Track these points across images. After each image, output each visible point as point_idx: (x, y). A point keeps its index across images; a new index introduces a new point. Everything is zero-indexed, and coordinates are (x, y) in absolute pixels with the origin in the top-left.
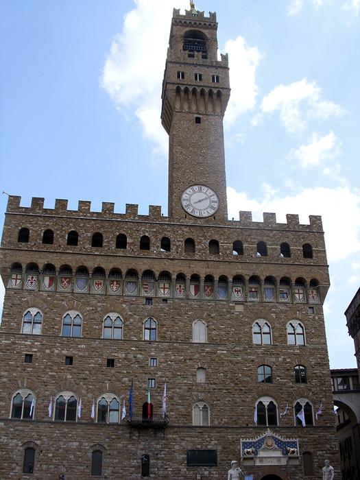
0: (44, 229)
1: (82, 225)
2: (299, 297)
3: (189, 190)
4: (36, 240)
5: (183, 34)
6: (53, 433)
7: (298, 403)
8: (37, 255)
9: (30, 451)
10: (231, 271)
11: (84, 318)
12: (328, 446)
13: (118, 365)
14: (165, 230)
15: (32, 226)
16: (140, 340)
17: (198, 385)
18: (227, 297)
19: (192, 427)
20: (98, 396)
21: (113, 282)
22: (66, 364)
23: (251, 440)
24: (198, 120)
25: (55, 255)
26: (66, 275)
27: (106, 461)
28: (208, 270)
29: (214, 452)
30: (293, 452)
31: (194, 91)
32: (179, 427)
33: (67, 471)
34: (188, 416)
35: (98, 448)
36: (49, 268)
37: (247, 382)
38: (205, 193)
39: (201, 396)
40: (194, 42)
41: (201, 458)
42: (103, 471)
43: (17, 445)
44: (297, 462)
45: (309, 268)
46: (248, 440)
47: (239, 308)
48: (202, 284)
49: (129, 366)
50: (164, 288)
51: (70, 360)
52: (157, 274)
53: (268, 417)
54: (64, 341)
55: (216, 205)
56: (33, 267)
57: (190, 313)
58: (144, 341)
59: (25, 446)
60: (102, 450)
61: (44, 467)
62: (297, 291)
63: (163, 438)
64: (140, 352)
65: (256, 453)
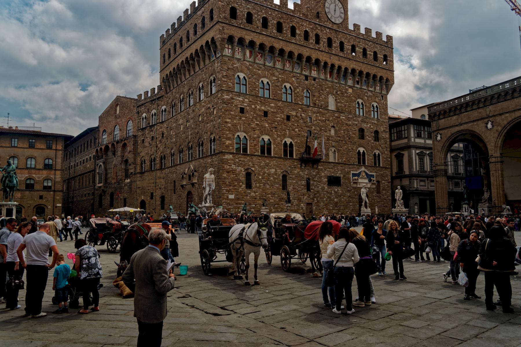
1: (270, 13)
2: (378, 88)
4: (242, 20)
6: (261, 163)
9: (248, 175)
10: (351, 65)
13: (293, 120)
14: (317, 28)
15: (239, 7)
19: (330, 163)
23: (355, 172)
25: (255, 34)
27: (289, 181)
28: (339, 62)
29: (340, 177)
30: (374, 181)
32: (323, 162)
34: (327, 155)
35: (285, 173)
36: (252, 44)
37: (354, 138)
41: (334, 181)
42: (288, 187)
43: (241, 171)
44: (374, 186)
45: (385, 71)
47: (350, 90)
48: (335, 71)
50: (314, 70)
51: (266, 114)
53: (361, 158)
55: (343, 16)
56: (241, 41)
58: (305, 105)
60: (287, 174)
61: (258, 185)
63: (317, 168)
65: (358, 179)
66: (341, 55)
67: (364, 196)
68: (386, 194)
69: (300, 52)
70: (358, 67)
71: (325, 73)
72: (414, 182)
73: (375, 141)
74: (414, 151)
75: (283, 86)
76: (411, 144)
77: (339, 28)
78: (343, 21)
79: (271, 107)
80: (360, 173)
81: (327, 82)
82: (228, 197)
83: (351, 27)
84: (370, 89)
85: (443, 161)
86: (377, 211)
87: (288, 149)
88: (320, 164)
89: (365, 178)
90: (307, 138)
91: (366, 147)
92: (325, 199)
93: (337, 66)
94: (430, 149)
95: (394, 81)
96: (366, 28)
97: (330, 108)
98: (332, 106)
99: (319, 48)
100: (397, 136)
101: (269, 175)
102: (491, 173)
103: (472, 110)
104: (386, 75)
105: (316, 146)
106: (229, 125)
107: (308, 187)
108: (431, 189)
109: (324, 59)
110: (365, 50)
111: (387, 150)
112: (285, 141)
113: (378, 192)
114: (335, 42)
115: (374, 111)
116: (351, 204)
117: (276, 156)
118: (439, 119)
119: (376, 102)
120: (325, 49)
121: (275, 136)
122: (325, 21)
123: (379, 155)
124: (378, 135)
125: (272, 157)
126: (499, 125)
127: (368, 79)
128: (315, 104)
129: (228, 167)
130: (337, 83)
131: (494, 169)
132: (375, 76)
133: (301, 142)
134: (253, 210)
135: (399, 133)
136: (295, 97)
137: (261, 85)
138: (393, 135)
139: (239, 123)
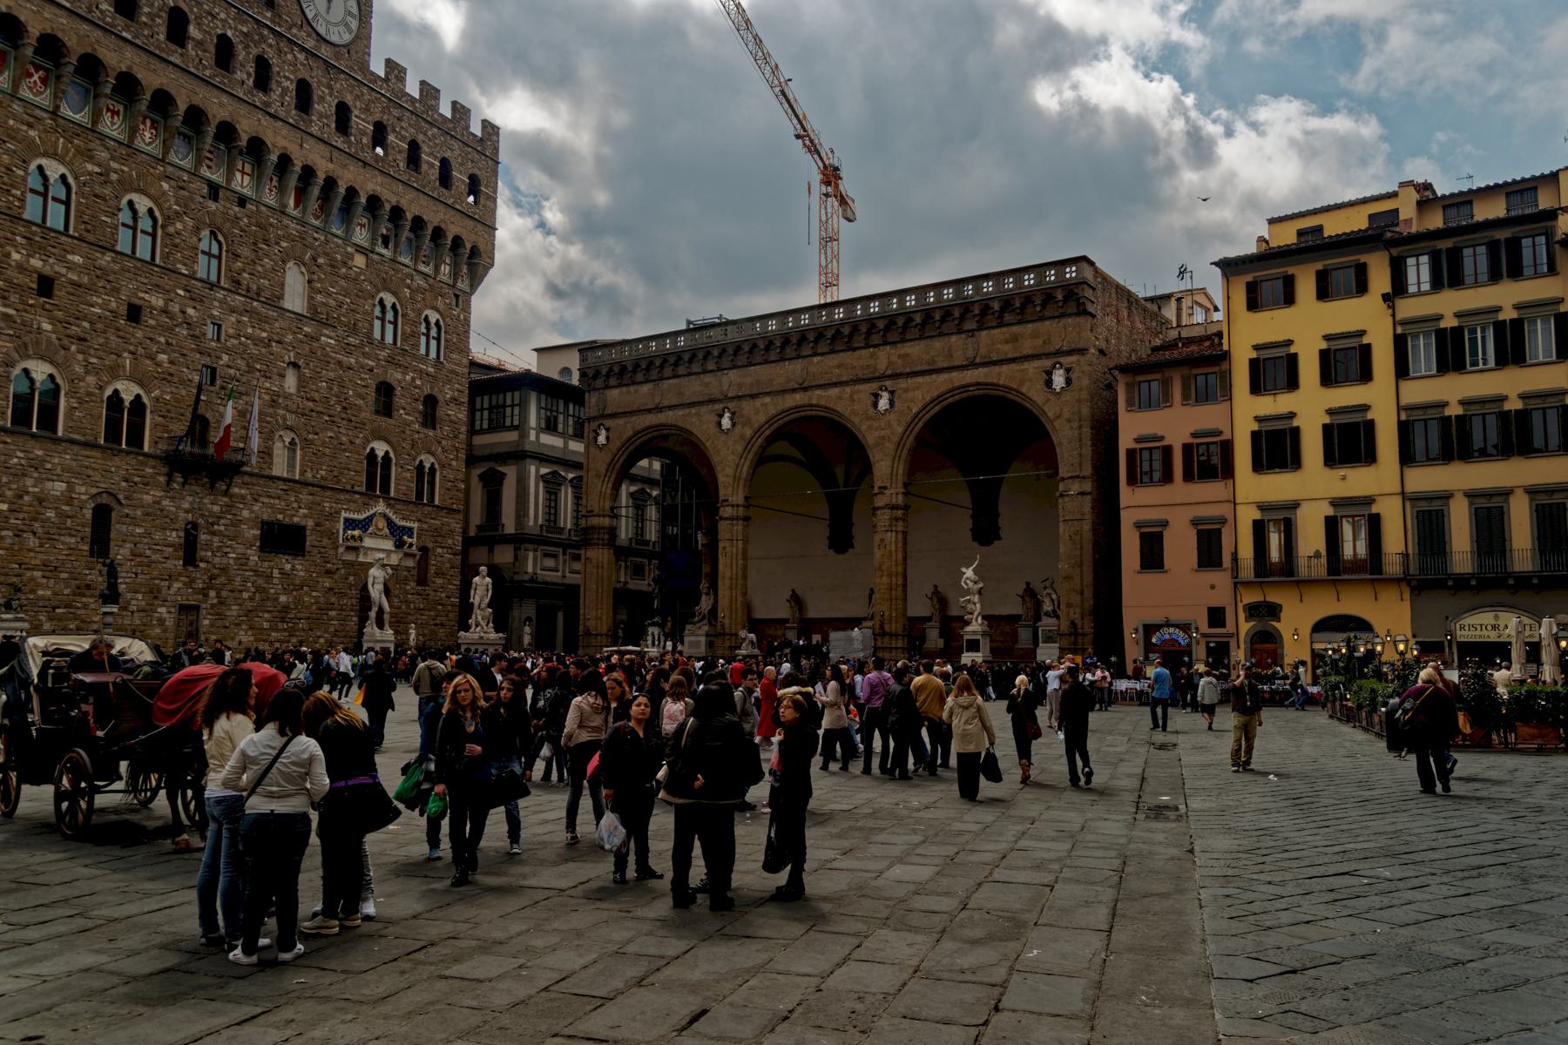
2: (445, 269)
6: (11, 456)
10: (370, 184)
11: (78, 186)
14: (263, 39)
16: (192, 277)
17: (288, 397)
18: (347, 231)
19: (272, 478)
20: (108, 383)
21: (145, 118)
27: (118, 529)
28: (331, 166)
29: (304, 528)
30: (411, 545)
32: (251, 475)
33: (41, 545)
34: (266, 454)
35: (105, 500)
37: (360, 408)
39: (291, 419)
41: (281, 539)
42: (113, 550)
44: (410, 563)
45: (471, 223)
46: (352, 516)
47: (360, 261)
48: (316, 191)
49: (170, 329)
50: (243, 173)
51: (46, 285)
53: (377, 474)
54: (34, 233)
55: (354, 24)
57: (284, 244)
60: (114, 505)
63: (226, 493)
64: (191, 303)
66: (339, 145)
67: (376, 592)
68: (444, 587)
69: (196, 101)
70: (391, 195)
71: (282, 190)
72: (526, 558)
73: (425, 425)
74: (533, 469)
75: (124, 202)
76: (527, 448)
77: (338, 60)
78: (352, 42)
79: (71, 267)
80: (370, 520)
81: (286, 221)
83: (378, 68)
84: (422, 268)
85: (608, 504)
86: (413, 636)
87: (123, 422)
88: (238, 480)
89: (385, 537)
90: (200, 389)
92: (245, 595)
93: (321, 176)
94: (577, 466)
95: (492, 259)
96: (423, 83)
97: (287, 305)
98: (295, 297)
99: (265, 103)
100: (490, 420)
101: (40, 501)
102: (721, 545)
103: (690, 374)
104: (473, 238)
105: (228, 419)
107: (190, 551)
108: (572, 579)
109: (282, 143)
110: (414, 147)
111: (457, 458)
112: (116, 392)
113: (422, 580)
114: (322, 99)
115: (427, 335)
116: (333, 613)
117: (76, 437)
118: (607, 387)
119: (438, 310)
120: (288, 112)
121: (78, 369)
122: (295, 25)
123: (432, 469)
124: (434, 409)
125: (60, 440)
126: (748, 422)
127: (418, 237)
128: (238, 283)
130: (317, 229)
131: (728, 536)
132: (438, 233)
133: (177, 401)
135: (497, 410)
136: (164, 245)
137: (34, 182)
138: (478, 414)
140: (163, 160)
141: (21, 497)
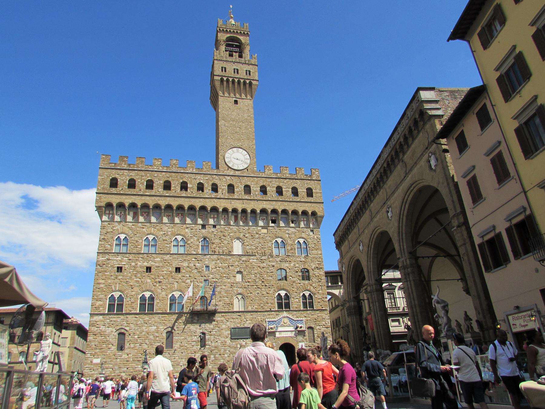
0: (128, 178)
1: (156, 175)
3: (230, 150)
5: (225, 38)
7: (304, 294)
8: (124, 197)
9: (122, 335)
12: (324, 323)
13: (184, 271)
19: (233, 312)
21: (179, 214)
22: (147, 272)
23: (273, 320)
24: (236, 102)
26: (146, 210)
30: (301, 327)
31: (233, 81)
36: (133, 206)
38: (241, 153)
40: (233, 45)
42: (174, 345)
46: (271, 320)
47: (265, 231)
51: (149, 269)
52: (209, 209)
55: (248, 161)
56: (121, 206)
59: (118, 332)
61: (132, 345)
62: (302, 219)
73: (303, 279)
77: (243, 173)
81: (231, 227)
82: (91, 362)
84: (292, 225)
89: (289, 326)
91: (288, 289)
106: (102, 286)
107: (203, 342)
119: (303, 238)
121: (160, 291)
122: (225, 170)
129: (96, 329)
134: (123, 374)
139: (113, 283)
140: (185, 224)
141: (141, 333)
